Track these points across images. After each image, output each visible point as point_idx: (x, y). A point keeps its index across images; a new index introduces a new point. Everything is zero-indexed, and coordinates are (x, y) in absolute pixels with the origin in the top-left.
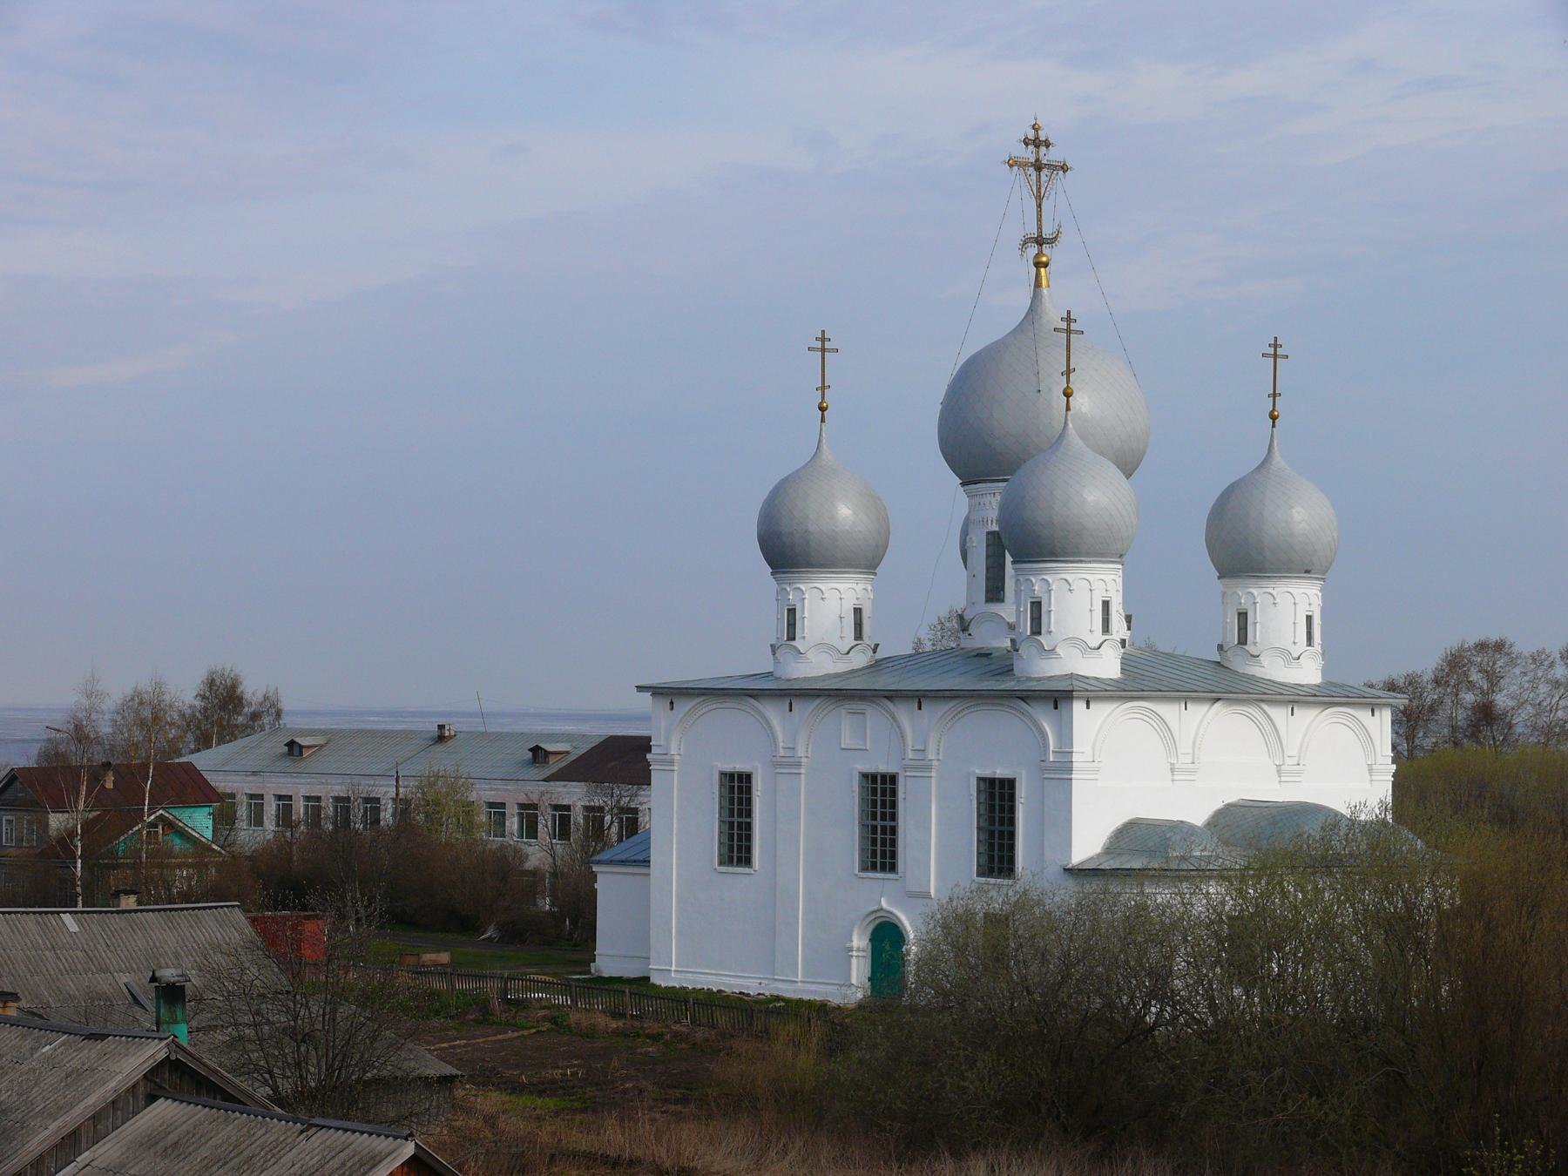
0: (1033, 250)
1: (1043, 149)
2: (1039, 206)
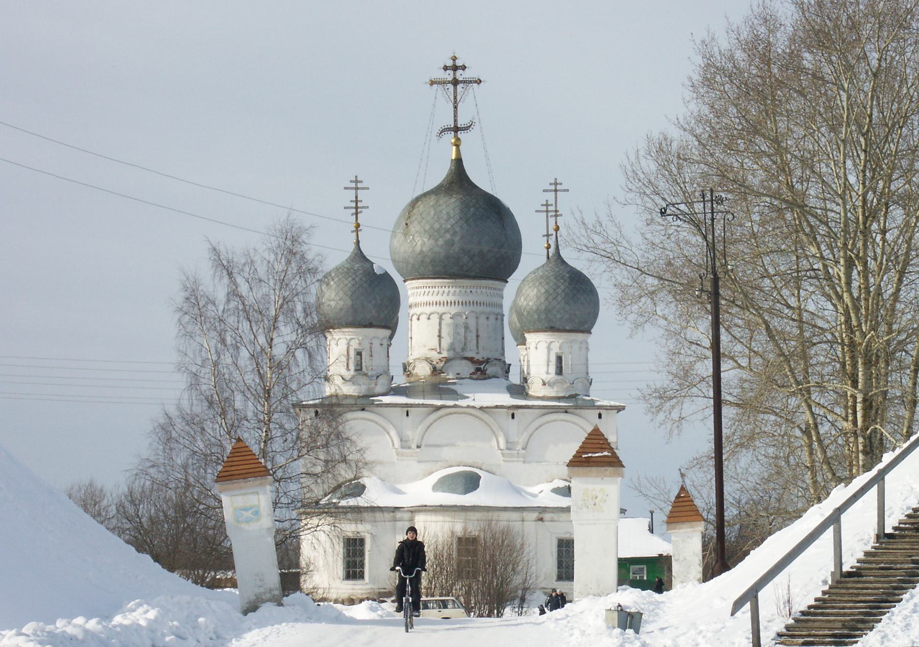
1: (459, 72)
2: (456, 107)
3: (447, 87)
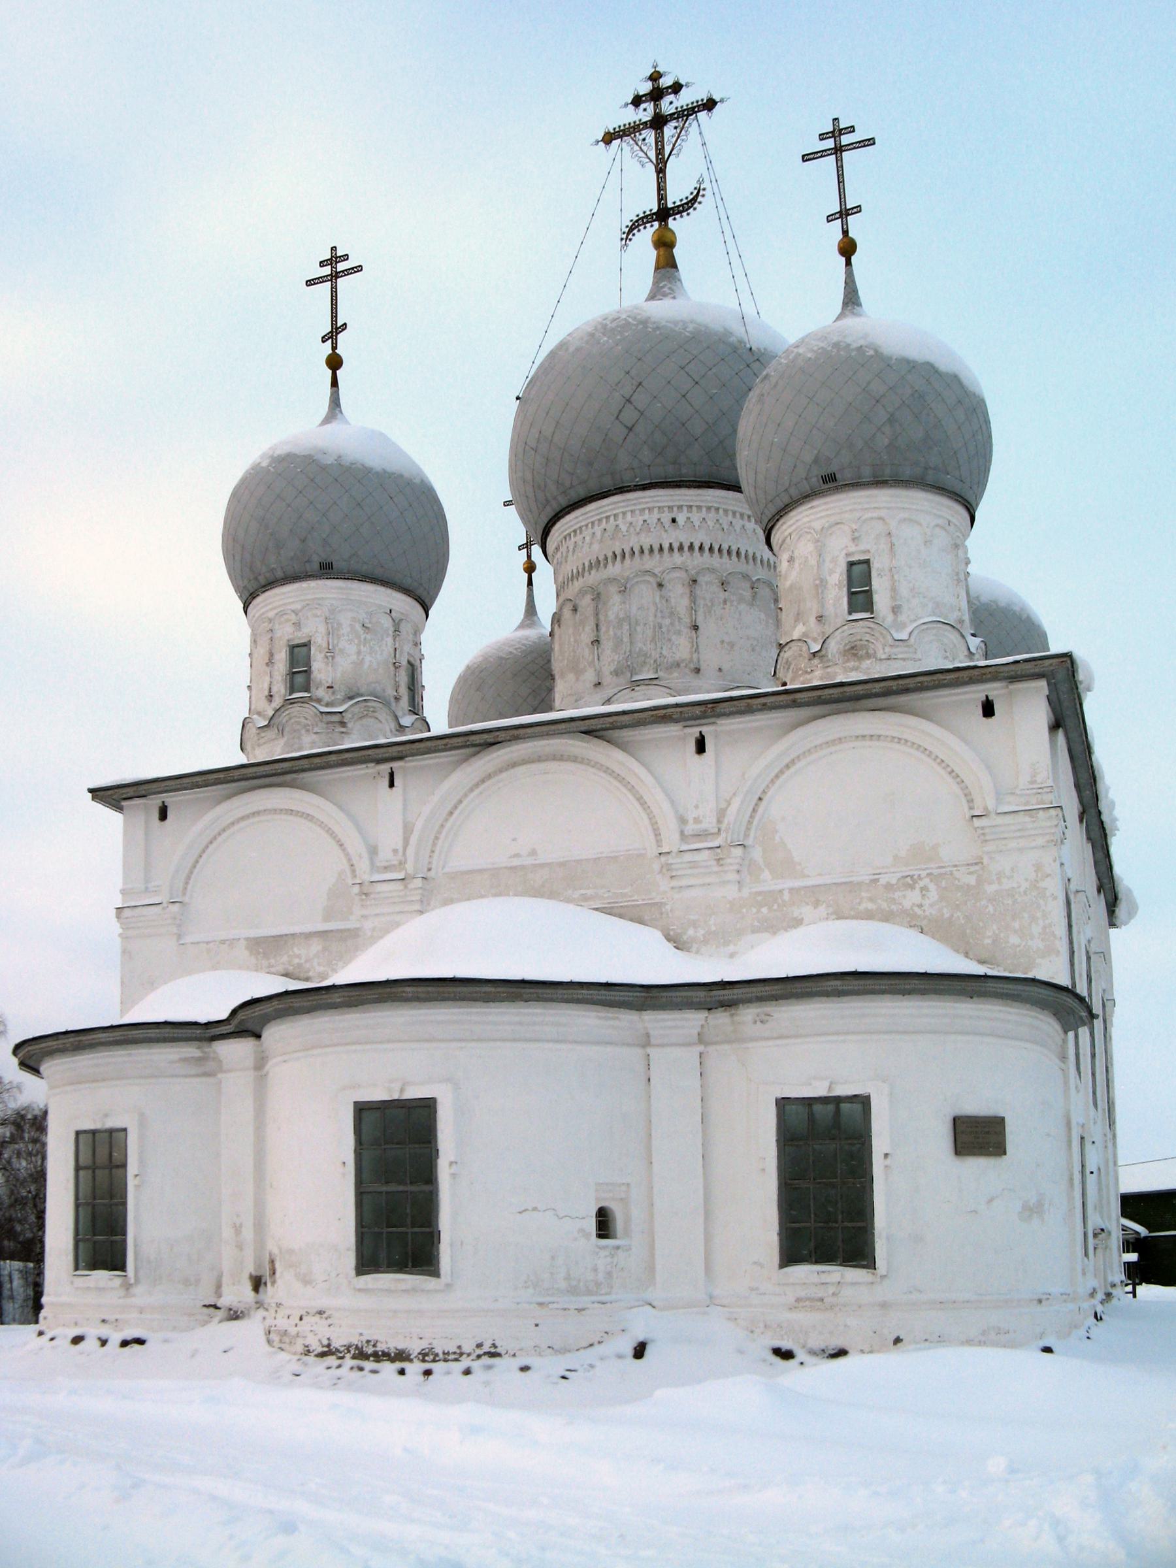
0: (647, 234)
2: (661, 171)
3: (641, 137)
